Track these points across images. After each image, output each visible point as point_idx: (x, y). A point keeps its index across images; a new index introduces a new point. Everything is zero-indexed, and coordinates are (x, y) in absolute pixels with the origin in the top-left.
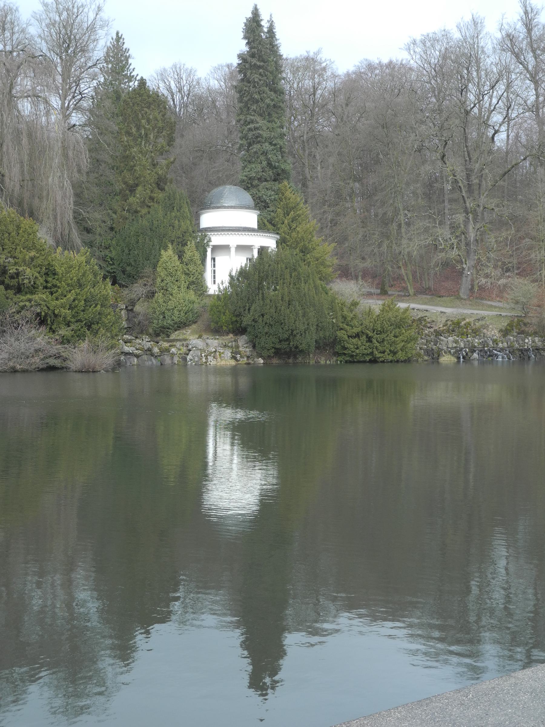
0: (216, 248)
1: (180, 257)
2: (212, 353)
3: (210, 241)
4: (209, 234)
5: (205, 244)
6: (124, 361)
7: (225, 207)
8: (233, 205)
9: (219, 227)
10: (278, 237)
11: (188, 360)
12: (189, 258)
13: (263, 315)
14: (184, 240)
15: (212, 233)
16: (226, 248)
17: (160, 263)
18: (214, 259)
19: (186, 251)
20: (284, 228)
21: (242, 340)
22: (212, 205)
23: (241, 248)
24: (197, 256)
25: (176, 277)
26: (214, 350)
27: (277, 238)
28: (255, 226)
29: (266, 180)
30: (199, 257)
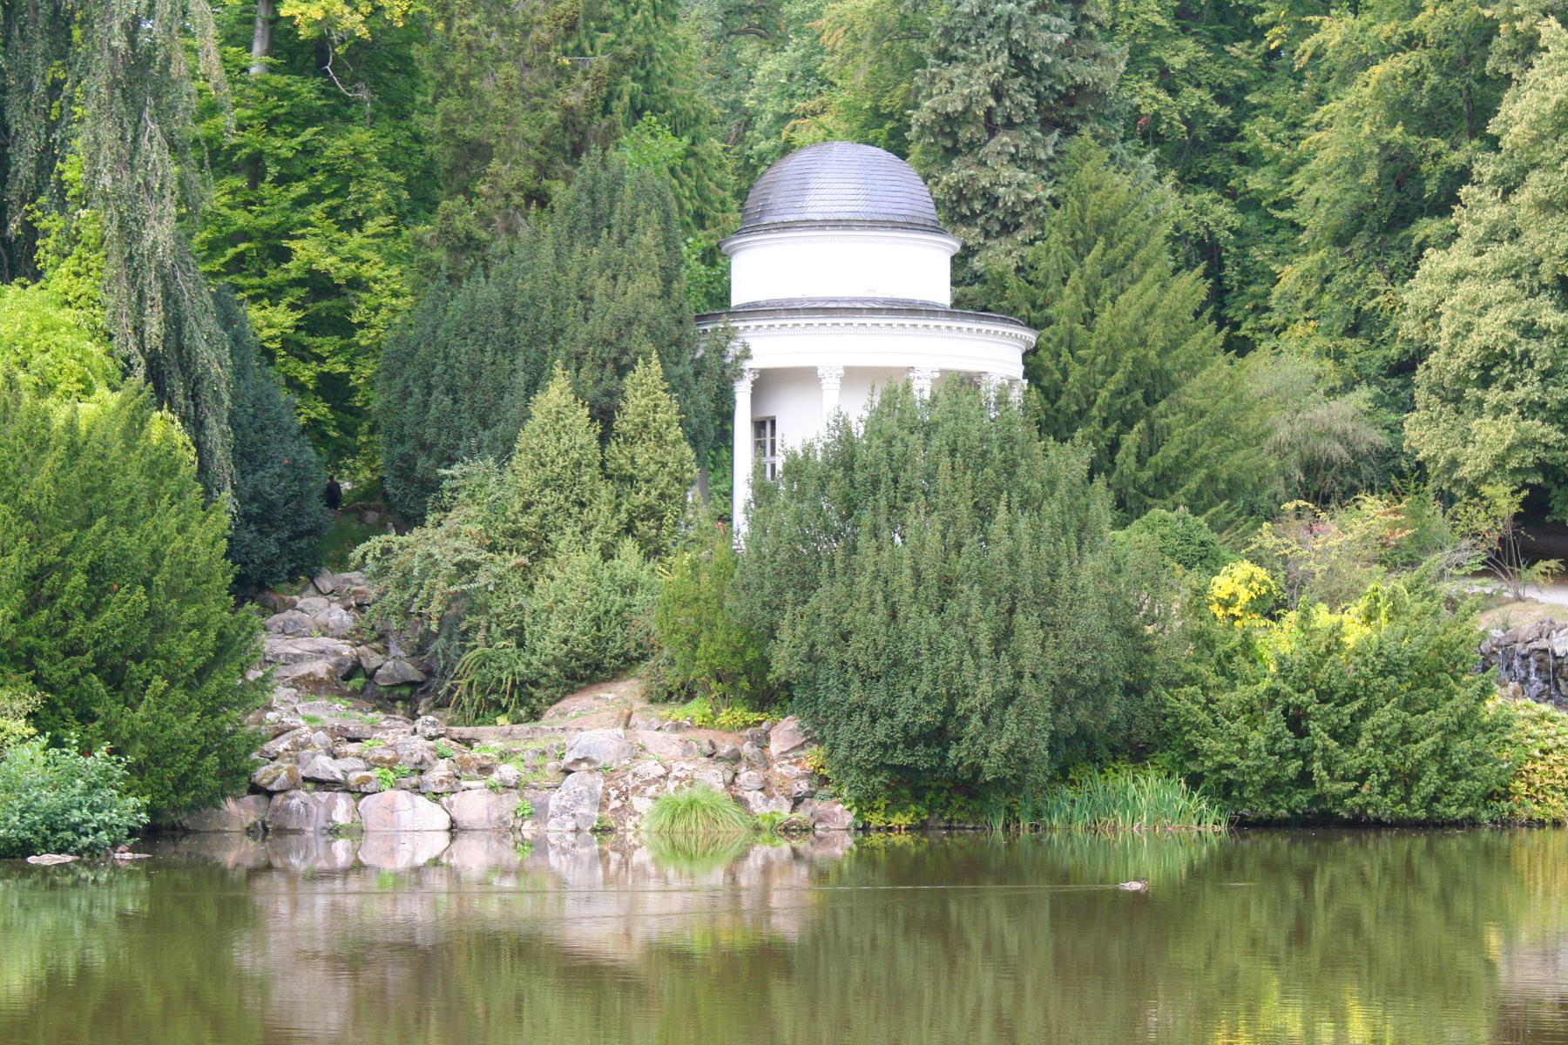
0: (765, 382)
1: (604, 415)
2: (649, 783)
3: (746, 354)
4: (741, 325)
5: (725, 366)
6: (302, 810)
7: (810, 224)
8: (845, 216)
9: (780, 302)
10: (1031, 336)
11: (552, 808)
12: (638, 420)
13: (845, 637)
14: (624, 352)
15: (753, 324)
16: (805, 377)
17: (522, 436)
18: (762, 426)
19: (629, 392)
20: (1067, 302)
21: (784, 731)
22: (767, 220)
23: (852, 376)
24: (668, 410)
25: (576, 489)
26: (662, 771)
27: (1028, 343)
28: (941, 292)
29: (1009, 124)
30: (679, 413)
